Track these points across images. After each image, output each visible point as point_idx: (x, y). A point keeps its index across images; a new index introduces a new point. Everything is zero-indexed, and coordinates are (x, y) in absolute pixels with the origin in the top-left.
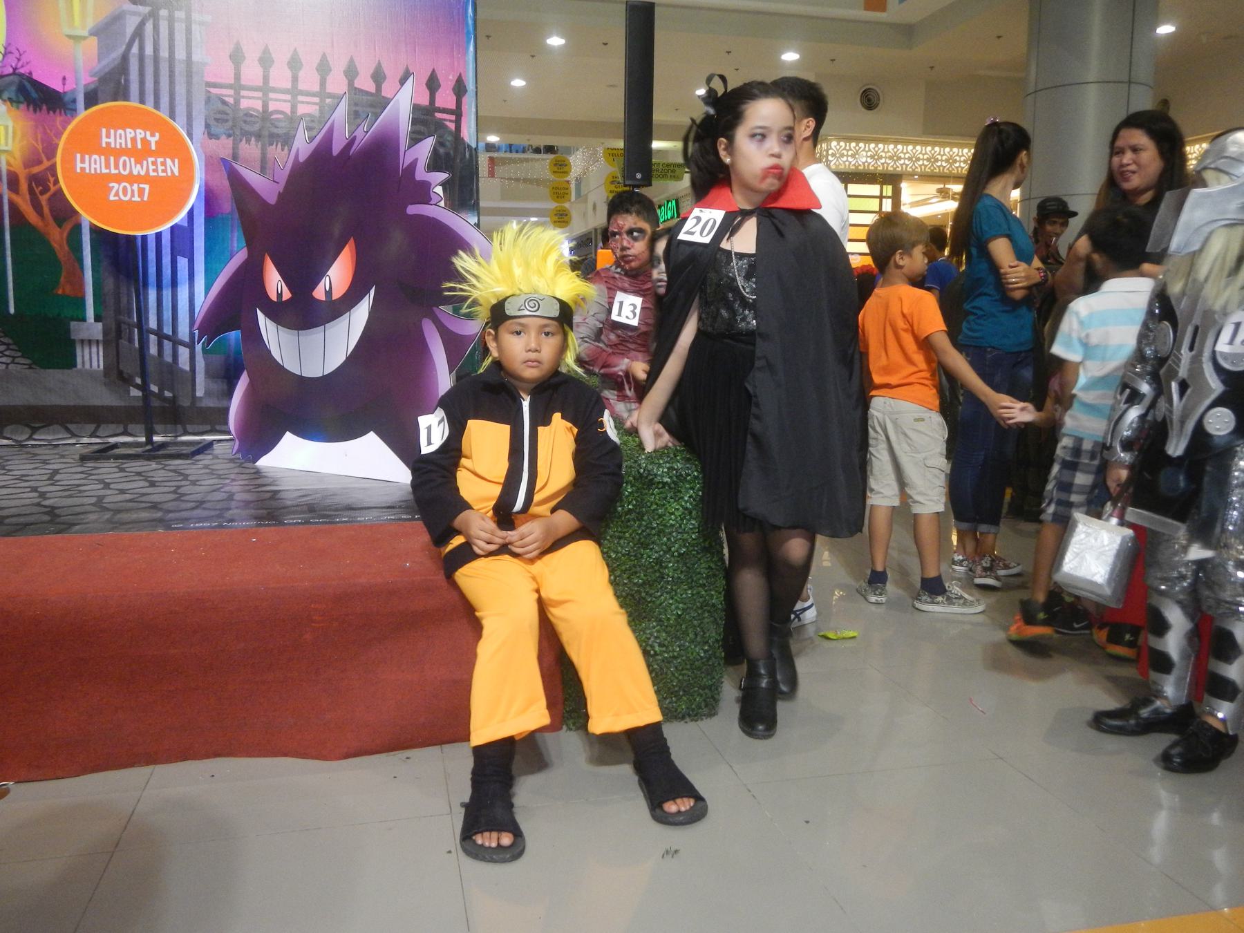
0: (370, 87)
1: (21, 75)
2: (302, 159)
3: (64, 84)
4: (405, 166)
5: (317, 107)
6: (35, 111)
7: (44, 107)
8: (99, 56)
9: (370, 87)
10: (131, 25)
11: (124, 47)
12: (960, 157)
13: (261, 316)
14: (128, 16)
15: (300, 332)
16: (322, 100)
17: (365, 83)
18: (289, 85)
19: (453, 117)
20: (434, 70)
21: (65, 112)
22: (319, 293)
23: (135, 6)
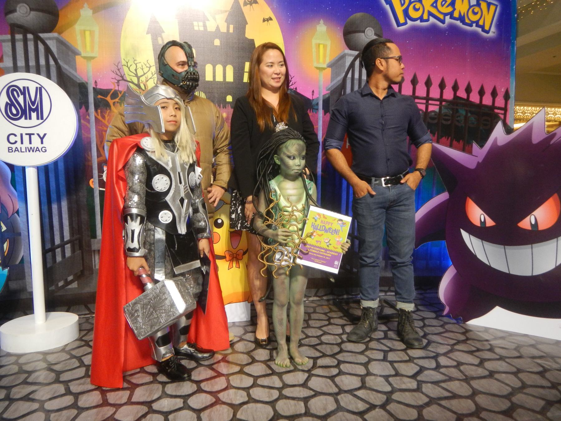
2: (500, 143)
3: (313, 95)
5: (438, 107)
8: (331, 79)
10: (349, 61)
11: (344, 74)
12: (528, 111)
13: (465, 235)
14: (347, 57)
15: (506, 247)
16: (441, 103)
17: (462, 94)
18: (425, 95)
19: (503, 112)
21: (312, 110)
22: (526, 224)
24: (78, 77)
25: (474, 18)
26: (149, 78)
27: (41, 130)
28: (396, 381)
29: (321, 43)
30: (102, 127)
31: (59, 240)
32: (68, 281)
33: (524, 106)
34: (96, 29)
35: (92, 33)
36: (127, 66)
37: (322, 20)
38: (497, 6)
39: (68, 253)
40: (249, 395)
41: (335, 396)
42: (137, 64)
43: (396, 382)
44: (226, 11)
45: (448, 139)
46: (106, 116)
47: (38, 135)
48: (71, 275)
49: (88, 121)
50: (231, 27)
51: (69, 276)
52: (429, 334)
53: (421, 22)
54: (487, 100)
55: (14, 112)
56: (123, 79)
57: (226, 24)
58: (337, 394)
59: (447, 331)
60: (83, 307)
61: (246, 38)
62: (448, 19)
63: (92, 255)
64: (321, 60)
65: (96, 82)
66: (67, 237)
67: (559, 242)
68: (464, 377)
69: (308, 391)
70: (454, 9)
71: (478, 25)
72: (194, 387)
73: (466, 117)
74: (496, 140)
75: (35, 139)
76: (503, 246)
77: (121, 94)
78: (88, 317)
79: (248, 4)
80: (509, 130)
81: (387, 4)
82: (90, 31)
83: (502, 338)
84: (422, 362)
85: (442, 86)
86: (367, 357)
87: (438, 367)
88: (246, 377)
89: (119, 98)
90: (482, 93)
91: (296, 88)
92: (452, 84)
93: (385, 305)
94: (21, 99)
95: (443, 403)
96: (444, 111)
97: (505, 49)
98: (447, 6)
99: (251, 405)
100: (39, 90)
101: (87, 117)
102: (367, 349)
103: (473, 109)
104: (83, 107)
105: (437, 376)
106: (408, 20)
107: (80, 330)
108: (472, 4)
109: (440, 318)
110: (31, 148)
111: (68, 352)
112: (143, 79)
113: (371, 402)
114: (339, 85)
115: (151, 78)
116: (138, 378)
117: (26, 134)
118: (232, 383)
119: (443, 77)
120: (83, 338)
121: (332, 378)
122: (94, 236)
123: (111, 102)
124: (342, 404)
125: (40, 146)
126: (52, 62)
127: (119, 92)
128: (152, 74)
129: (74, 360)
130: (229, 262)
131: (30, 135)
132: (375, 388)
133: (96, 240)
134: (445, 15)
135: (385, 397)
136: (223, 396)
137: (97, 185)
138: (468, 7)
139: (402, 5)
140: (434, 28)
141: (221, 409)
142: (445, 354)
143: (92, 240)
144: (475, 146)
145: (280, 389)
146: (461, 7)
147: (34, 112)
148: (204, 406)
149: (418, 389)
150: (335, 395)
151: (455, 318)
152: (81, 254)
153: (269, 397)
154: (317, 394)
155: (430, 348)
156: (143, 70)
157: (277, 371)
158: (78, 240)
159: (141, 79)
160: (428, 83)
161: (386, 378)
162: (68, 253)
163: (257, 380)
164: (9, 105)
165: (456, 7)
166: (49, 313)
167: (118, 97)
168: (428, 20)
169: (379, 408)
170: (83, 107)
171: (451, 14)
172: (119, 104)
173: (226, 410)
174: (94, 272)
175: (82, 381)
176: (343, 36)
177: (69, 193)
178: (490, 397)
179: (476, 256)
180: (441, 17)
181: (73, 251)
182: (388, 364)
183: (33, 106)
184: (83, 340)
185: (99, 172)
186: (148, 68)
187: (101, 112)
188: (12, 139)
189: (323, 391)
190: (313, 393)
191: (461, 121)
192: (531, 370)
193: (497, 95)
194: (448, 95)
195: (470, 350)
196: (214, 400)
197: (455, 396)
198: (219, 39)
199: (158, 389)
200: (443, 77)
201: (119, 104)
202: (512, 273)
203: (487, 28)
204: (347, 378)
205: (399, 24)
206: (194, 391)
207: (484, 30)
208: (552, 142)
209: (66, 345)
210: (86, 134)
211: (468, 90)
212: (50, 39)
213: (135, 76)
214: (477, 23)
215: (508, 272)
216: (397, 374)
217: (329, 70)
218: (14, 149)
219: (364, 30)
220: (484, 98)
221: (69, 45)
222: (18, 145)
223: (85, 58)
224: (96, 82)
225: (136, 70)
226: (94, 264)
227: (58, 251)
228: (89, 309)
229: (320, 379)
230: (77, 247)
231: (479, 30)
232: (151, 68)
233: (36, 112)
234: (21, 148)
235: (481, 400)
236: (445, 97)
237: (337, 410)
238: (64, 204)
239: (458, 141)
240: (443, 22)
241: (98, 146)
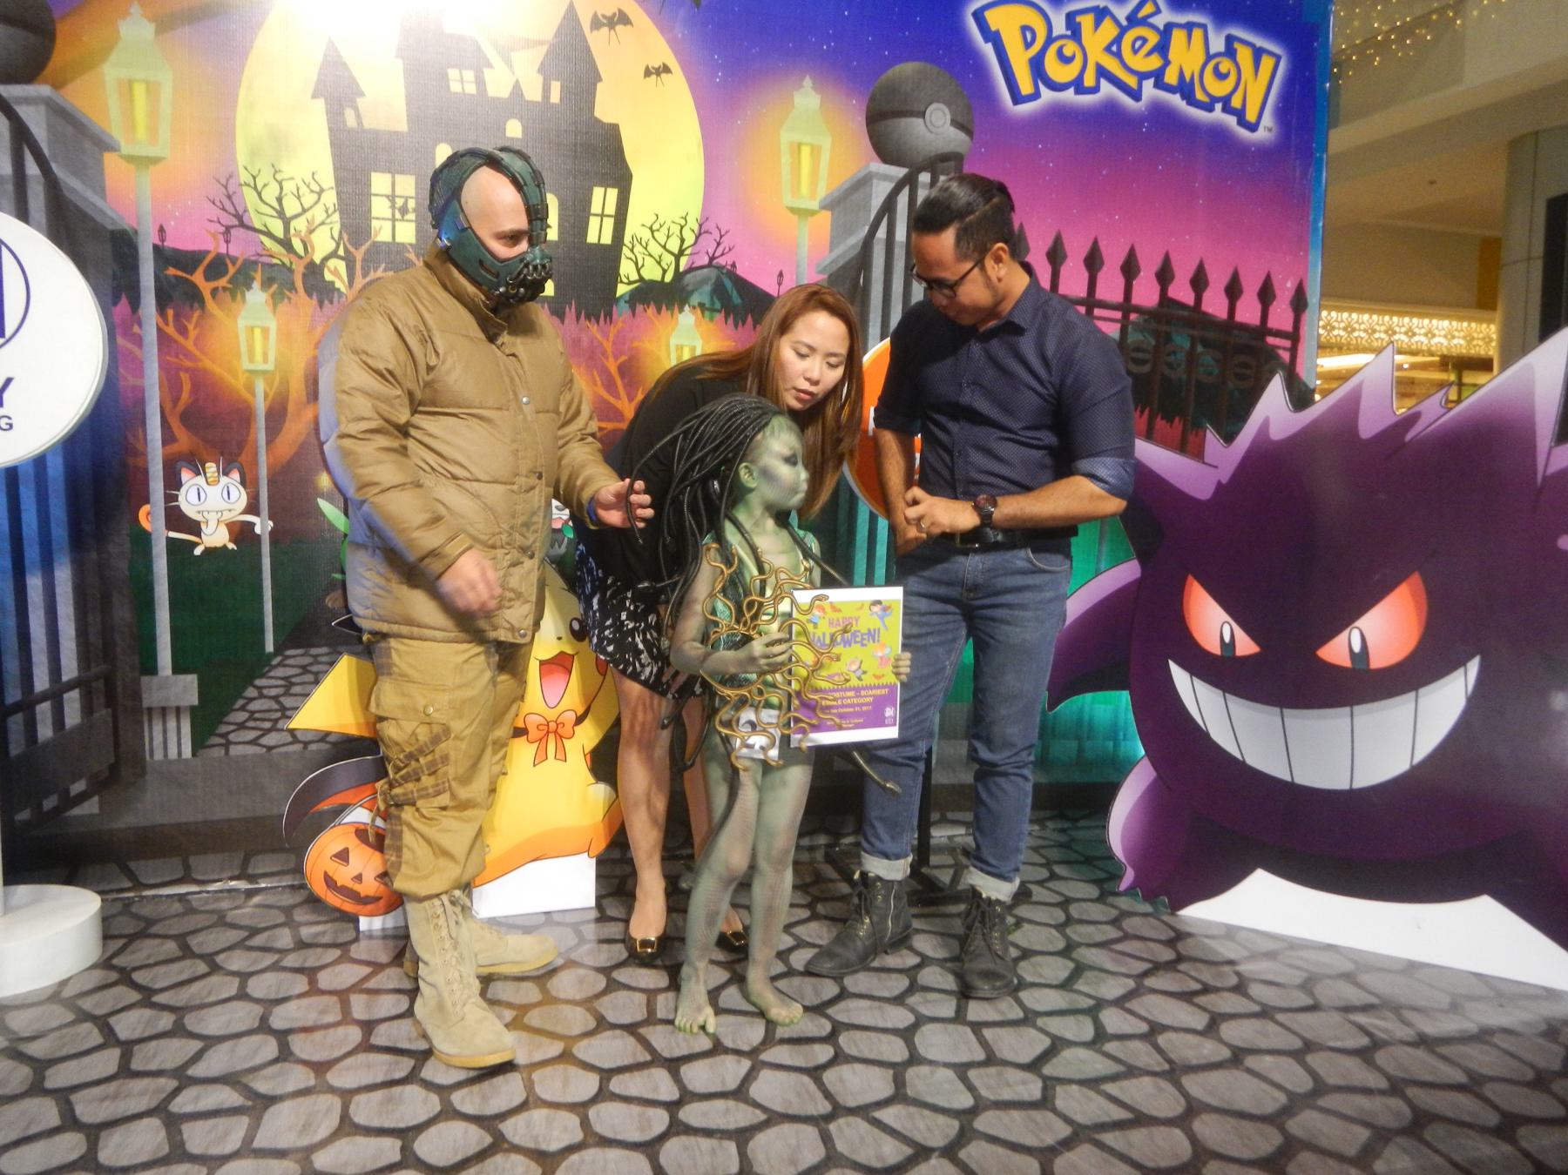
0: (1187, 296)
1: (720, 268)
2: (1278, 433)
3: (779, 284)
4: (1552, 469)
5: (1119, 325)
6: (736, 326)
7: (750, 319)
8: (832, 242)
9: (1187, 296)
11: (867, 228)
13: (1180, 676)
14: (875, 181)
15: (1286, 711)
16: (1126, 317)
17: (1182, 292)
18: (1083, 294)
19: (1288, 343)
20: (1268, 277)
23: (887, 166)
24: (109, 213)
25: (1219, 89)
26: (317, 223)
28: (986, 1080)
29: (804, 141)
30: (177, 357)
31: (46, 678)
32: (73, 793)
33: (1351, 310)
34: (166, 79)
35: (153, 90)
36: (255, 188)
37: (808, 77)
38: (1278, 58)
39: (73, 717)
40: (585, 1124)
41: (822, 1124)
42: (284, 183)
43: (988, 1083)
44: (541, 43)
45: (1142, 412)
46: (190, 327)
48: (80, 778)
49: (138, 341)
50: (556, 88)
51: (73, 782)
52: (1080, 945)
53: (1077, 92)
54: (1248, 312)
56: (242, 225)
57: (539, 79)
58: (829, 1118)
59: (1126, 937)
60: (114, 868)
61: (598, 121)
62: (1148, 86)
63: (142, 723)
64: (805, 188)
65: (162, 230)
66: (70, 670)
67: (1421, 701)
68: (1167, 1067)
69: (750, 1109)
70: (1167, 63)
71: (1227, 109)
72: (434, 1104)
73: (1191, 357)
74: (1265, 426)
76: (1277, 710)
77: (234, 264)
78: (128, 898)
79: (604, 25)
80: (1300, 397)
81: (986, 40)
82: (147, 82)
83: (1271, 955)
84: (1057, 1026)
85: (1130, 269)
86: (912, 1010)
87: (1100, 1037)
88: (580, 1072)
89: (227, 278)
90: (1233, 291)
91: (734, 265)
92: (1156, 265)
93: (964, 860)
95: (1108, 1138)
96: (1134, 337)
97: (1298, 173)
98: (1149, 54)
99: (591, 1154)
101: (136, 329)
102: (913, 988)
103: (1210, 335)
104: (124, 301)
105: (1096, 1065)
106: (1042, 88)
107: (107, 937)
108: (1212, 51)
109: (1111, 899)
111: (70, 1004)
112: (299, 225)
113: (918, 1138)
114: (850, 261)
115: (323, 223)
116: (273, 1077)
118: (538, 1090)
119: (1132, 250)
120: (115, 961)
121: (815, 1072)
122: (151, 668)
123: (205, 288)
124: (841, 1146)
126: (32, 169)
127: (228, 261)
128: (327, 212)
129: (88, 1026)
130: (536, 745)
132: (930, 1100)
133: (155, 680)
134: (1142, 76)
135: (956, 1124)
136: (514, 1129)
137: (161, 522)
138: (1201, 58)
139: (1028, 45)
140: (1111, 108)
141: (508, 1166)
142: (1119, 1002)
143: (145, 679)
144: (1212, 439)
145: (672, 1107)
146: (1186, 56)
148: (459, 1157)
149: (1044, 1102)
150: (820, 1122)
151: (1150, 896)
152: (110, 720)
153: (642, 1129)
154: (774, 1118)
155: (1080, 985)
156: (299, 198)
157: (666, 1054)
158: (102, 681)
159: (293, 224)
160: (1093, 262)
161: (961, 1070)
162: (73, 717)
163: (609, 1079)
165: (1172, 55)
166: (13, 888)
167: (227, 272)
168: (1095, 90)
169: (940, 1156)
170: (124, 301)
171: (1158, 76)
172: (228, 293)
173: (520, 1169)
174: (149, 769)
175: (111, 1087)
176: (864, 122)
177: (77, 542)
178: (1232, 1121)
179: (1207, 735)
180: (1132, 81)
181: (88, 709)
182: (968, 1030)
184: (112, 968)
185: (166, 487)
186: (315, 197)
187: (177, 316)
189: (790, 1112)
190: (763, 1117)
191: (1179, 365)
192: (1338, 1044)
193: (1274, 297)
194: (1146, 293)
195: (1186, 989)
196: (488, 1140)
197: (1140, 1120)
198: (521, 119)
199: (329, 1110)
200: (1132, 250)
201: (228, 293)
202: (1299, 780)
203: (1251, 116)
204: (854, 1073)
205: (1017, 98)
206: (431, 1115)
207: (1242, 122)
208: (1409, 437)
209: (63, 983)
210: (130, 378)
211: (1199, 282)
212: (28, 101)
213: (275, 214)
214: (1226, 101)
215: (1289, 779)
216: (991, 1060)
217: (826, 217)
219: (922, 109)
220: (1240, 305)
221: (84, 120)
223: (130, 159)
224: (162, 230)
225: (279, 200)
226: (147, 747)
227: (44, 709)
228: (132, 876)
229: (782, 1075)
230: (100, 700)
231: (1231, 121)
232: (324, 196)
235: (1209, 1129)
236: (1137, 299)
237: (826, 1165)
238: (64, 576)
239: (1170, 420)
240: (1136, 95)
241: (167, 411)
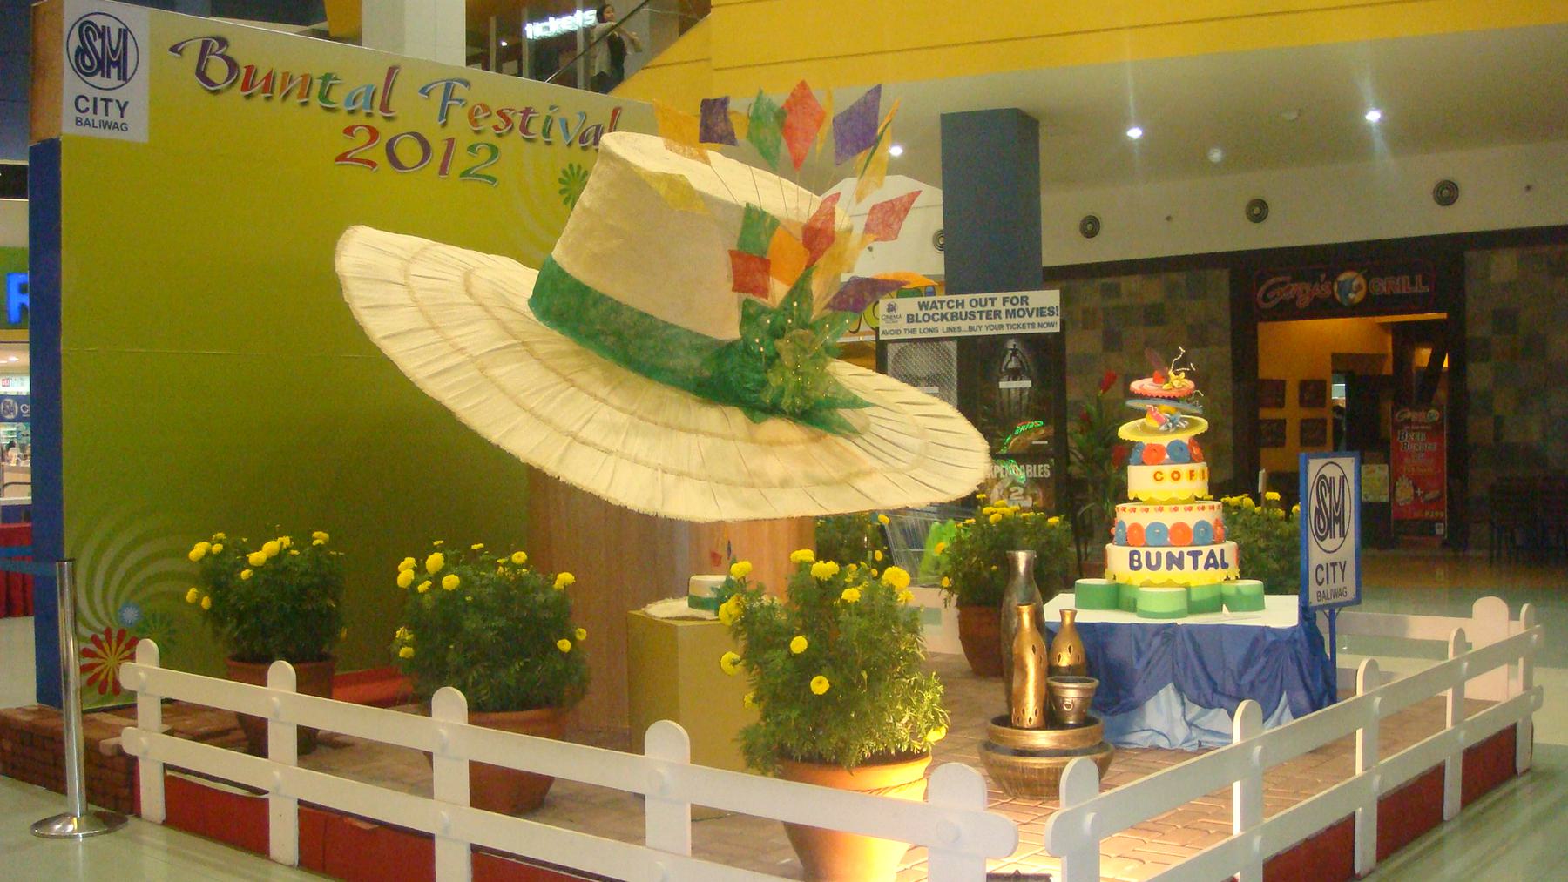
27: (120, 95)
47: (117, 101)
55: (88, 63)
75: (113, 108)
94: (98, 44)
100: (124, 33)
110: (107, 122)
117: (102, 99)
125: (120, 121)
131: (107, 101)
147: (114, 67)
164: (81, 52)
183: (114, 56)
188: (82, 104)
218: (83, 122)
222: (90, 115)
233: (116, 69)
234: (93, 121)
